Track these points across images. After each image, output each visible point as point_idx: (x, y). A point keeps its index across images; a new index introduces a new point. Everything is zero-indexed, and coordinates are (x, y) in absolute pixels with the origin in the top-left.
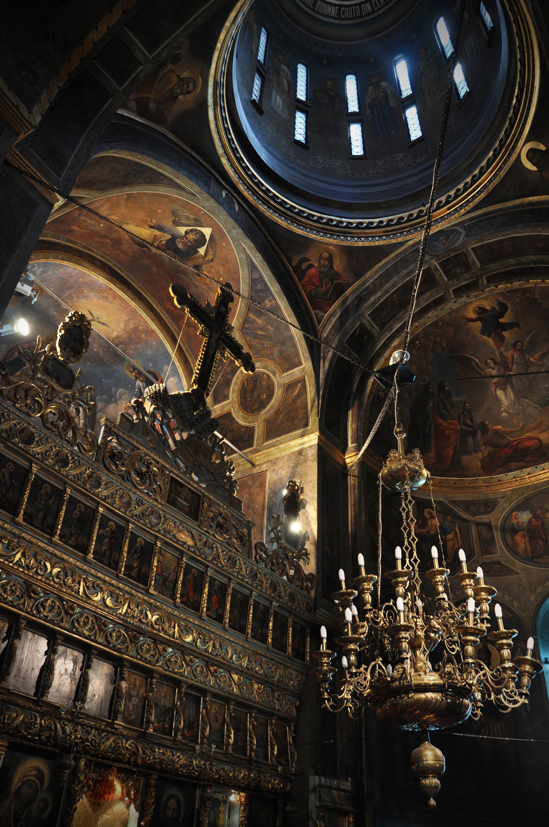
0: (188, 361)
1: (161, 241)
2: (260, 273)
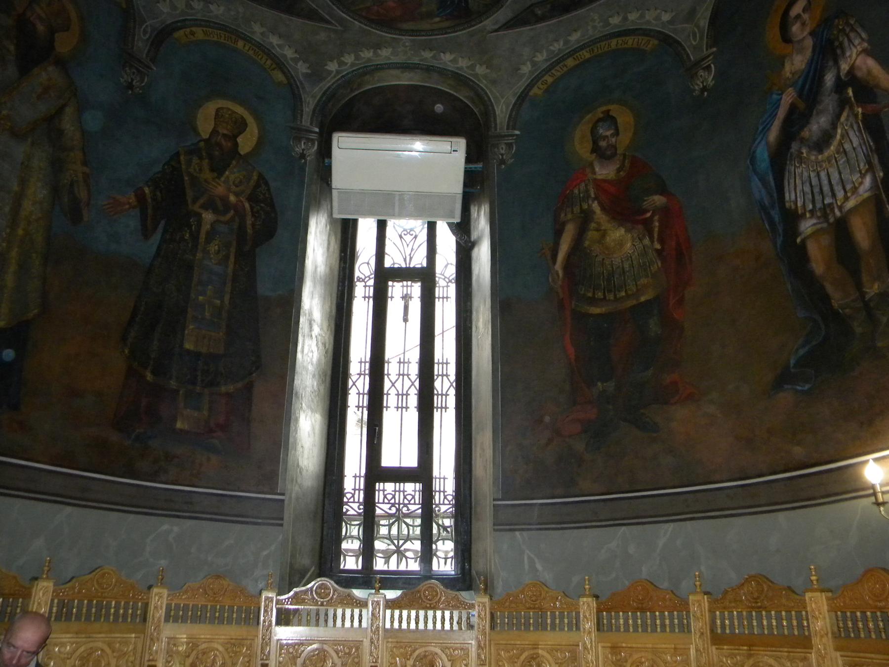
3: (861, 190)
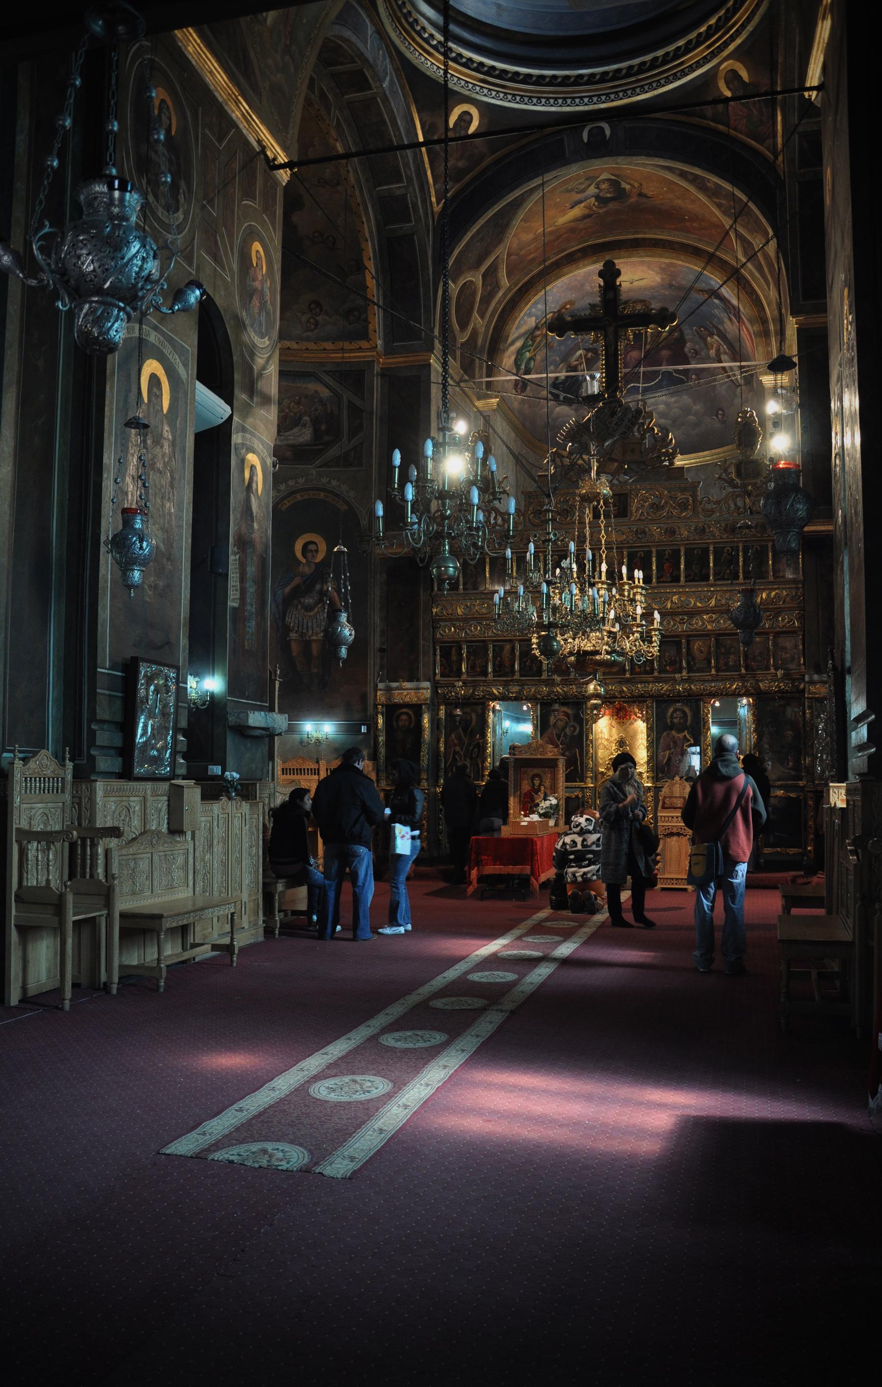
0: (726, 262)
1: (594, 205)
2: (677, 168)
3: (319, 635)
